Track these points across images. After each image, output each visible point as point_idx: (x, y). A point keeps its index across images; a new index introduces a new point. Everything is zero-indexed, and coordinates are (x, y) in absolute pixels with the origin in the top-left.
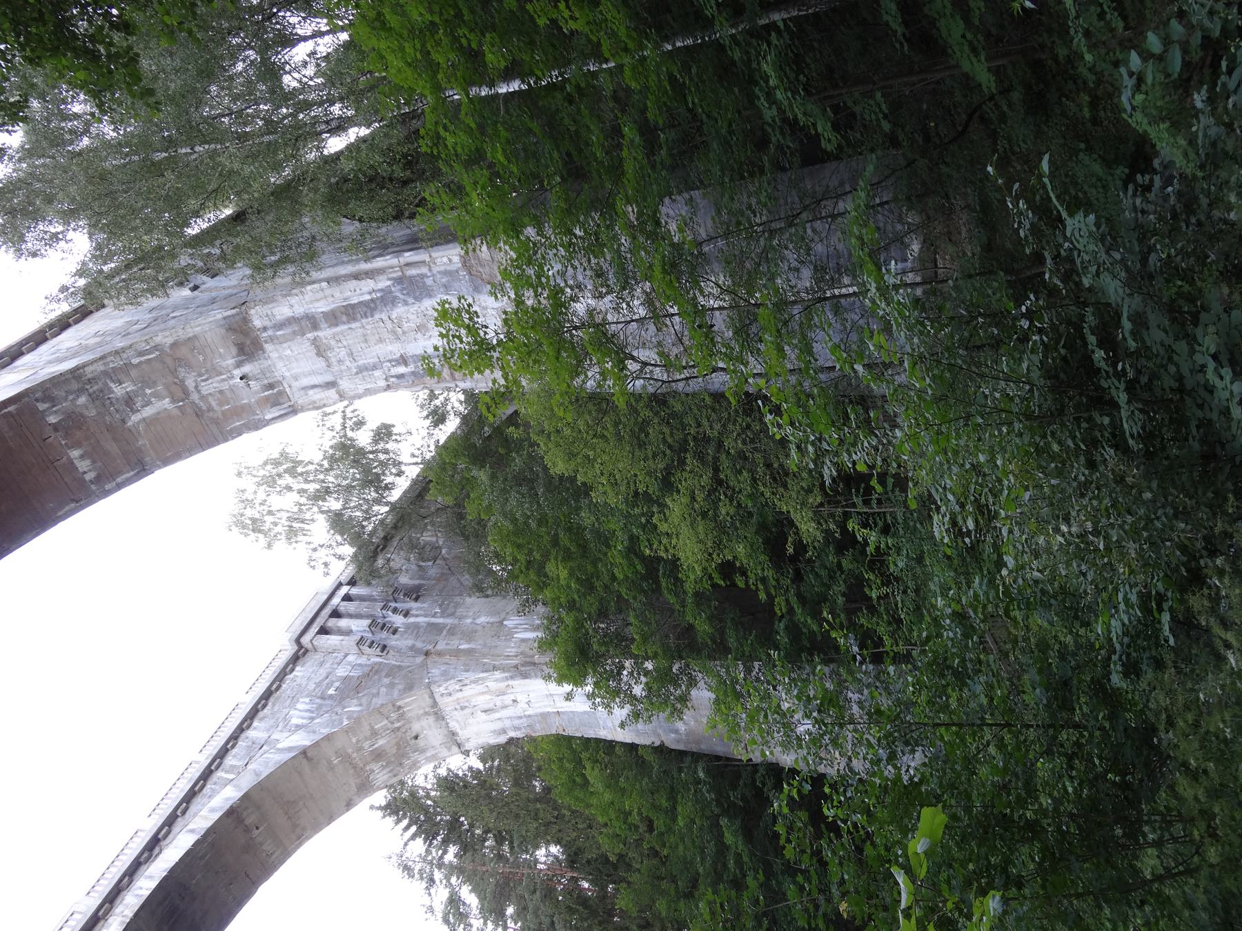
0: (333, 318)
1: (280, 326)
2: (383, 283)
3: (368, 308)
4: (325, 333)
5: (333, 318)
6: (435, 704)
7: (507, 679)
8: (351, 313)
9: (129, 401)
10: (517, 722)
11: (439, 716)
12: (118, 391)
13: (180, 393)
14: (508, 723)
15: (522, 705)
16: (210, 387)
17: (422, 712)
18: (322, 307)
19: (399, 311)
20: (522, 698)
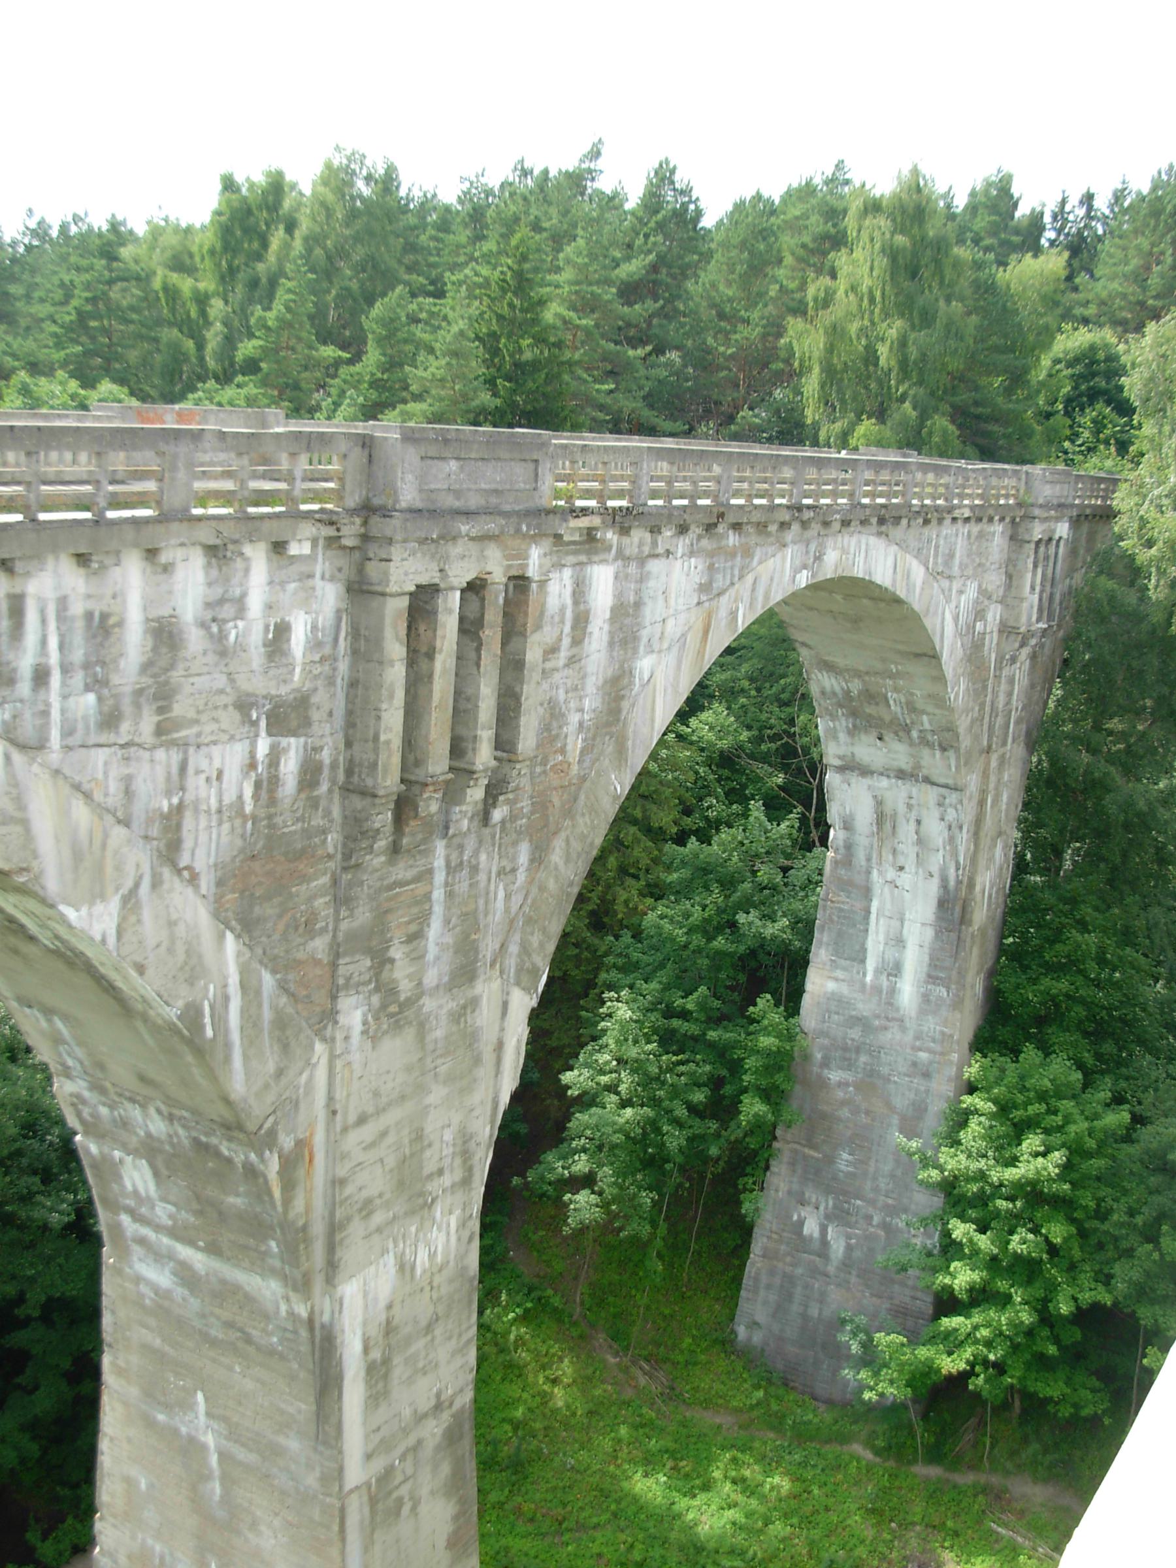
6: (927, 780)
7: (944, 880)
11: (901, 775)
15: (891, 874)
17: (923, 763)
20: (905, 880)
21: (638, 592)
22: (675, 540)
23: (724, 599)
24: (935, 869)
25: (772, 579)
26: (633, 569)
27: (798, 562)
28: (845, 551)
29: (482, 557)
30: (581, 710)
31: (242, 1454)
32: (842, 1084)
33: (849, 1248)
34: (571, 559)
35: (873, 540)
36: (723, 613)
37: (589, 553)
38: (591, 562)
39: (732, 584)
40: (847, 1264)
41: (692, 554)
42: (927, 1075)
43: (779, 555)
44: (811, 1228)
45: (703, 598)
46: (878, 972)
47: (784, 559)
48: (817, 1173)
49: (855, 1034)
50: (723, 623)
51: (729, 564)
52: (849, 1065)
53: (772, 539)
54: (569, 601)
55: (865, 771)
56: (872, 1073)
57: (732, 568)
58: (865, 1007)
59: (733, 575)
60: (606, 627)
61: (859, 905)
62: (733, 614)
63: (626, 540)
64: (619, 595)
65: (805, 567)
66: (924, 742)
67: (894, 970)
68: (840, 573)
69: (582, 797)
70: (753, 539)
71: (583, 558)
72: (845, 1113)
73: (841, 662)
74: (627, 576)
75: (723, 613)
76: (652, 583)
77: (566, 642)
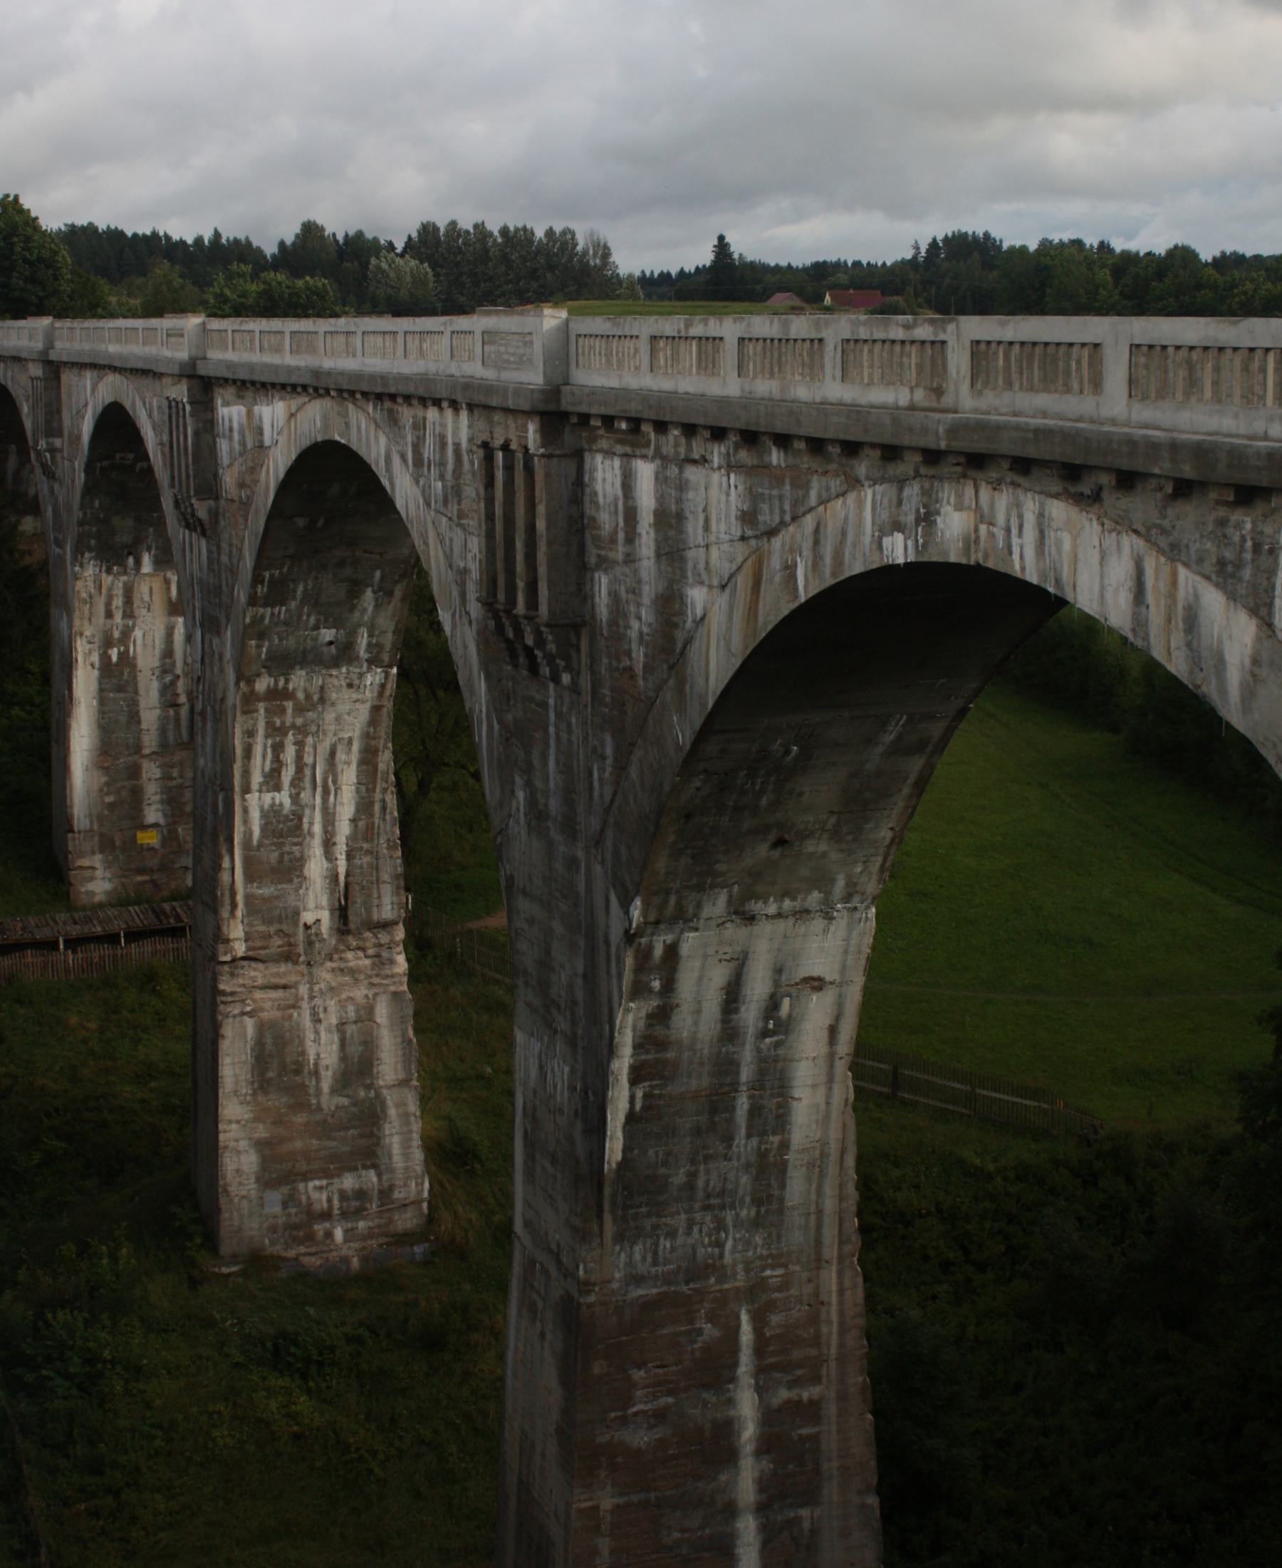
21: (679, 501)
22: (709, 445)
23: (777, 542)
25: (844, 533)
26: (673, 471)
27: (885, 516)
28: (984, 517)
29: (507, 427)
30: (639, 618)
34: (619, 449)
35: (1059, 510)
36: (776, 562)
37: (633, 445)
38: (635, 456)
39: (783, 524)
41: (730, 467)
43: (851, 497)
45: (749, 533)
47: (860, 503)
50: (778, 578)
51: (775, 492)
53: (834, 466)
54: (620, 493)
57: (781, 498)
59: (783, 512)
60: (652, 532)
62: (790, 569)
63: (663, 439)
64: (660, 499)
65: (898, 527)
68: (976, 557)
69: (651, 722)
70: (806, 462)
71: (628, 449)
74: (666, 479)
75: (776, 562)
76: (691, 495)
77: (621, 536)
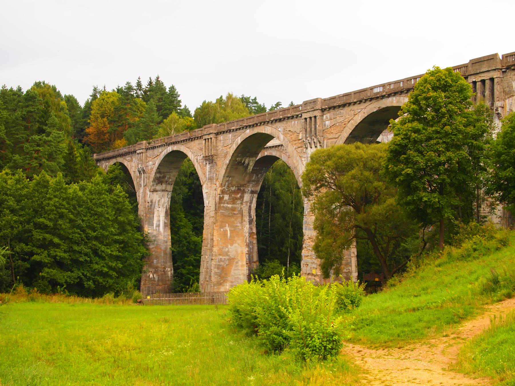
0: (250, 207)
1: (253, 198)
2: (252, 217)
3: (250, 213)
4: (248, 204)
5: (250, 207)
6: (167, 191)
8: (250, 209)
9: (258, 175)
10: (153, 206)
11: (163, 191)
12: (260, 175)
13: (254, 181)
14: (154, 204)
16: (251, 185)
18: (252, 206)
19: (248, 218)
20: (160, 209)
24: (165, 206)
31: (232, 229)
32: (153, 248)
33: (158, 278)
40: (158, 280)
42: (166, 242)
44: (151, 276)
46: (156, 227)
48: (151, 265)
49: (154, 238)
52: (153, 244)
55: (157, 191)
56: (157, 244)
58: (155, 233)
61: (152, 216)
66: (169, 184)
67: (158, 226)
72: (154, 253)
73: (162, 171)
